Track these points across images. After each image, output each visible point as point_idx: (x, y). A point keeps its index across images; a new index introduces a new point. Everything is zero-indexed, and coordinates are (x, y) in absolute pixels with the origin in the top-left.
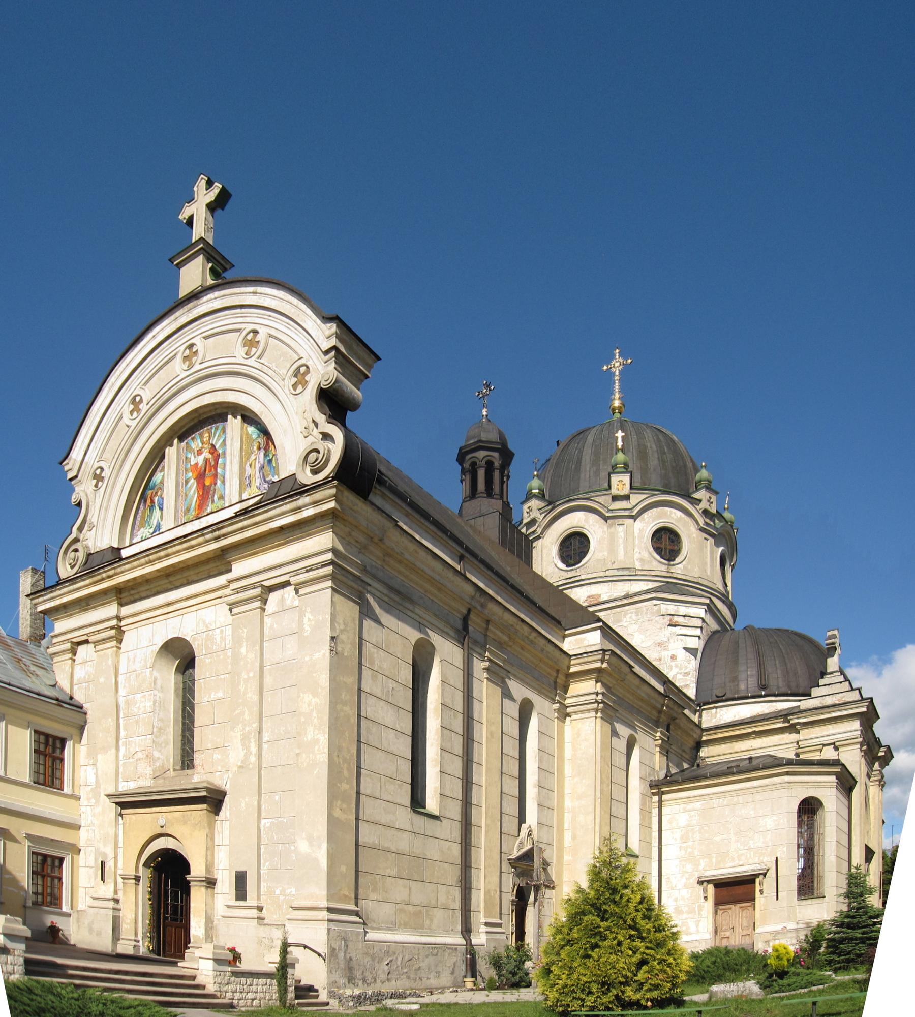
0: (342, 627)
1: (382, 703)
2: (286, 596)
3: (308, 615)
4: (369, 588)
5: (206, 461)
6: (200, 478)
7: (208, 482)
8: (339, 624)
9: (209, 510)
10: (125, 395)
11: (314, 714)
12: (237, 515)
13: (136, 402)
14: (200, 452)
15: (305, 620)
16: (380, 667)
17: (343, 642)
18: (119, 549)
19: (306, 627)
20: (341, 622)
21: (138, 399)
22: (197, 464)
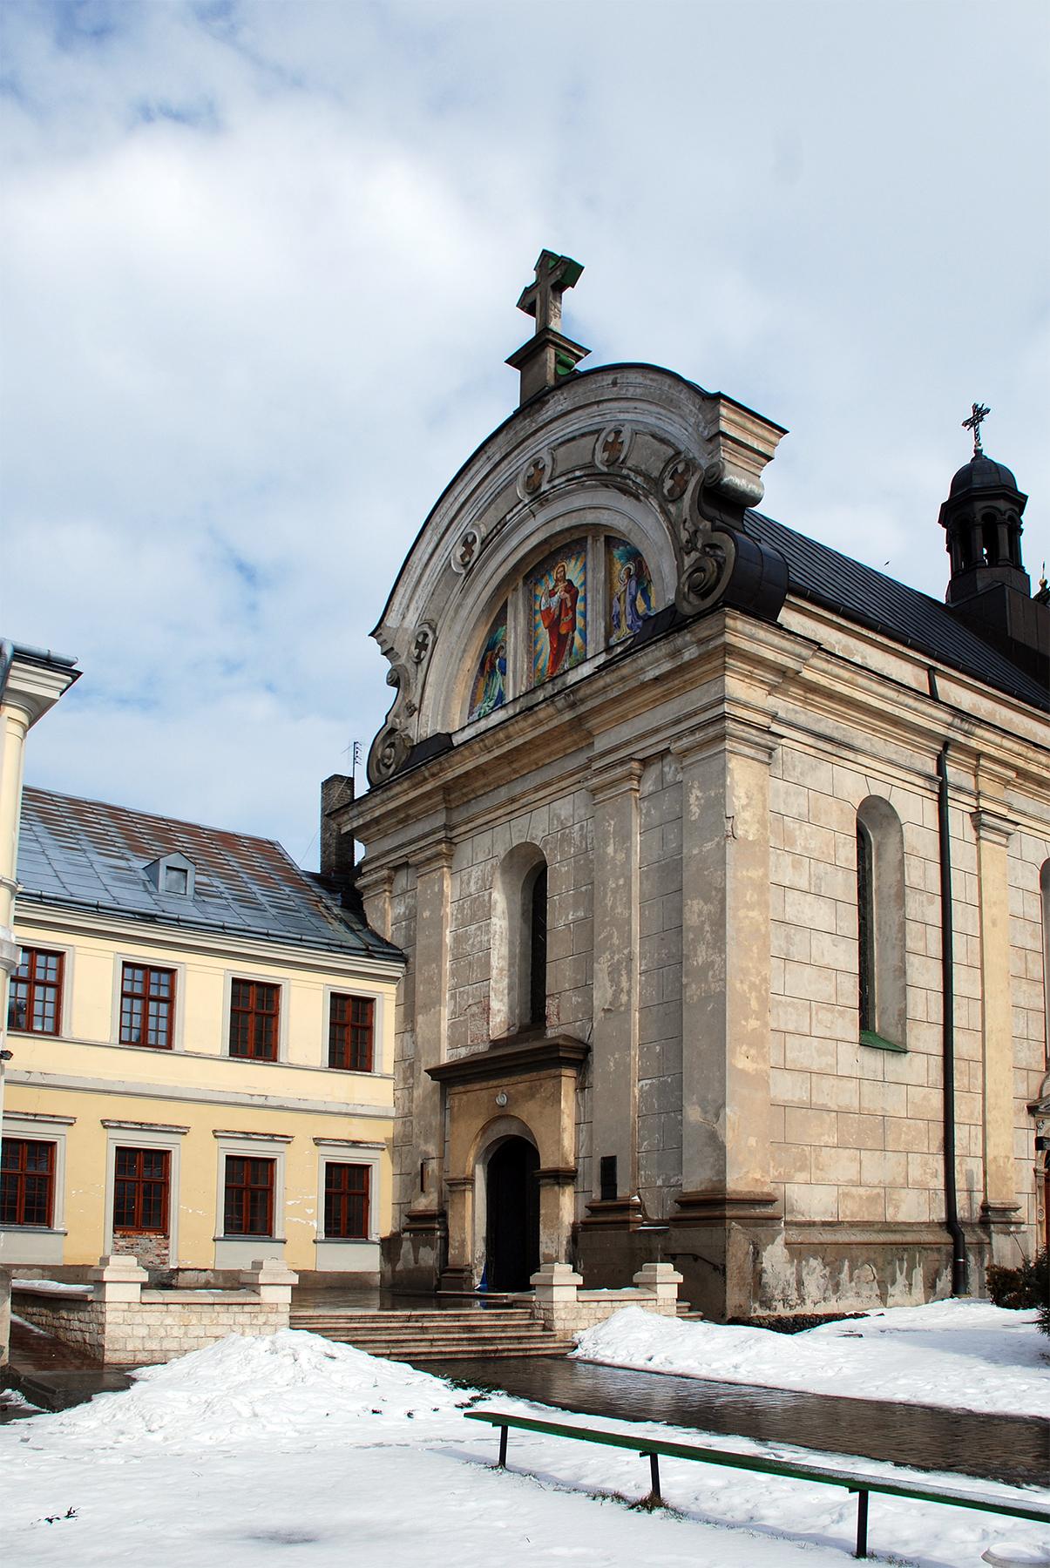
0: (744, 801)
1: (809, 898)
2: (666, 769)
3: (696, 792)
4: (783, 741)
5: (562, 602)
6: (553, 627)
7: (563, 632)
8: (738, 798)
9: (567, 666)
10: (454, 537)
11: (707, 928)
12: (600, 668)
13: (467, 544)
14: (552, 594)
15: (692, 800)
16: (806, 848)
17: (746, 822)
18: (450, 735)
19: (694, 809)
20: (742, 795)
21: (470, 539)
22: (549, 609)
